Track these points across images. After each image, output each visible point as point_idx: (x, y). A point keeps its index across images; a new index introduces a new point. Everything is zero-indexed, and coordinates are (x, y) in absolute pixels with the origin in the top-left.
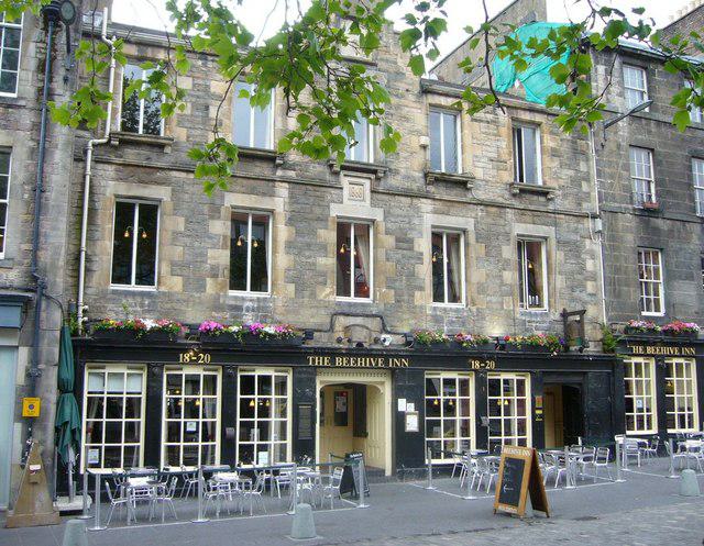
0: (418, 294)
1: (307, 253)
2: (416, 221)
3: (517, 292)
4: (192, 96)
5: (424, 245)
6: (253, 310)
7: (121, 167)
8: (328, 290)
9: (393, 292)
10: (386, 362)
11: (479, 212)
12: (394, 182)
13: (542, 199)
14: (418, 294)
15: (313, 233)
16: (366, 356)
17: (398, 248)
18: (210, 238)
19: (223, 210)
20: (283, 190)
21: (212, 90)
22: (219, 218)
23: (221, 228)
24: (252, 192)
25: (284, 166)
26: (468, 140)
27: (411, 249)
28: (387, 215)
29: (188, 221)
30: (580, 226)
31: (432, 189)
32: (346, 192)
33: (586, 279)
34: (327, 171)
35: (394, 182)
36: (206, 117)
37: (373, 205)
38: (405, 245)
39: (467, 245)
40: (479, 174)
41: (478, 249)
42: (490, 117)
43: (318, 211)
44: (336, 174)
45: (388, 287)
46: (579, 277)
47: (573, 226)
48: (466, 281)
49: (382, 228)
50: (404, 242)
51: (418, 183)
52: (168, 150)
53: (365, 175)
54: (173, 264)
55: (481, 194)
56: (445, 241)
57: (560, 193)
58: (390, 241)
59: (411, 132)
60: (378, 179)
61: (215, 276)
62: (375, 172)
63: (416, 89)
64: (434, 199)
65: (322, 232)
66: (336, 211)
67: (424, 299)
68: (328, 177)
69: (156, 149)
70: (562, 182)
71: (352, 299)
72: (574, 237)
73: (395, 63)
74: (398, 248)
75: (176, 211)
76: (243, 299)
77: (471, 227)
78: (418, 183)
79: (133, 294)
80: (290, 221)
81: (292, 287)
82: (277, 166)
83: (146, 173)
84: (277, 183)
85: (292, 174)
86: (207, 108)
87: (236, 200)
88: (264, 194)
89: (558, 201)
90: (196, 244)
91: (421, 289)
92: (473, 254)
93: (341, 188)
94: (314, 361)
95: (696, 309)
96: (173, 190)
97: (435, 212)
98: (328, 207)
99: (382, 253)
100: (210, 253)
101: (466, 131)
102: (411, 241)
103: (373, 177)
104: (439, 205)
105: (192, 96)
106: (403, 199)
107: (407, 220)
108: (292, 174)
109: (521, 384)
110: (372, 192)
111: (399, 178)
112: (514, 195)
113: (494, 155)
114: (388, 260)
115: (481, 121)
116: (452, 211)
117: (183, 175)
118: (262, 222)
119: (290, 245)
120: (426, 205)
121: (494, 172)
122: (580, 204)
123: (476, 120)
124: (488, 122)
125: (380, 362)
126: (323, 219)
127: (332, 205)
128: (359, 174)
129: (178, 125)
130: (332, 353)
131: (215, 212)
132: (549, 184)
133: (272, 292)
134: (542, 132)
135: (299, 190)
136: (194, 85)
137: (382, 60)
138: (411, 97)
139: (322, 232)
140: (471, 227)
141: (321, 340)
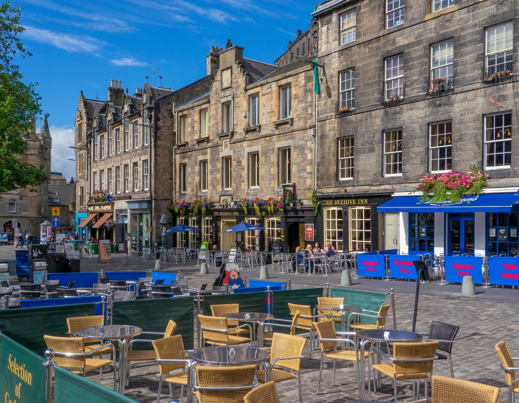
3: (276, 177)
12: (237, 137)
14: (243, 184)
27: (241, 165)
28: (234, 152)
30: (305, 135)
33: (307, 165)
36: (194, 130)
37: (231, 149)
42: (269, 90)
43: (216, 156)
46: (303, 164)
55: (264, 132)
56: (254, 156)
57: (296, 119)
70: (298, 113)
72: (302, 142)
89: (295, 124)
91: (244, 182)
95: (374, 172)
97: (248, 146)
102: (240, 162)
111: (238, 134)
113: (269, 110)
116: (254, 144)
120: (245, 144)
124: (268, 94)
138: (242, 96)
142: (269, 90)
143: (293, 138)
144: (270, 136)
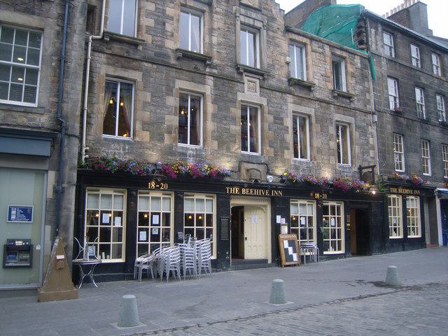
0: (286, 151)
1: (225, 122)
2: (284, 107)
4: (156, 15)
5: (289, 122)
6: (193, 156)
7: (110, 57)
8: (237, 146)
9: (272, 149)
10: (270, 193)
11: (317, 105)
12: (272, 82)
13: (348, 101)
14: (286, 151)
15: (228, 110)
16: (259, 188)
17: (275, 123)
18: (166, 108)
19: (174, 91)
20: (210, 81)
21: (167, 13)
22: (172, 95)
23: (173, 101)
24: (192, 80)
25: (211, 66)
26: (310, 62)
27: (282, 124)
29: (152, 96)
31: (292, 89)
32: (246, 85)
34: (235, 71)
35: (272, 82)
37: (261, 95)
38: (279, 122)
39: (311, 124)
40: (316, 82)
41: (317, 127)
43: (230, 96)
44: (241, 74)
45: (270, 147)
47: (363, 117)
48: (310, 145)
49: (266, 110)
50: (279, 119)
51: (285, 85)
52: (140, 48)
53: (257, 76)
54: (144, 123)
55: (317, 95)
56: (301, 121)
58: (270, 118)
59: (281, 54)
60: (264, 79)
61: (170, 133)
62: (262, 75)
63: (282, 28)
64: (294, 95)
65: (233, 109)
66: (240, 97)
67: (289, 154)
68: (236, 75)
69: (133, 47)
71: (249, 152)
73: (272, 12)
74: (275, 123)
75: (145, 88)
76: (187, 149)
77: (313, 114)
78: (285, 85)
79: (118, 142)
80: (214, 102)
81: (216, 143)
82: (206, 66)
83: (126, 61)
84: (207, 77)
85: (215, 71)
86: (164, 24)
87: (182, 84)
88: (199, 83)
89: (355, 103)
90: (158, 111)
91: (288, 149)
92: (314, 130)
93: (244, 83)
94: (230, 190)
96: (143, 75)
97: (294, 103)
98: (236, 94)
99: (266, 125)
100: (167, 117)
101: (309, 57)
102: (282, 119)
103: (261, 78)
104: (296, 99)
105: (156, 15)
106: (277, 93)
107: (279, 106)
108: (215, 71)
109: (339, 208)
110: (261, 87)
112: (334, 97)
114: (270, 129)
115: (316, 52)
117: (150, 65)
118: (196, 100)
119: (214, 116)
120: (290, 98)
121: (323, 83)
122: (365, 106)
123: (314, 51)
125: (267, 193)
126: (234, 101)
127: (238, 93)
128: (254, 76)
129: (146, 33)
130: (241, 186)
131: (170, 91)
132: (350, 92)
133: (204, 145)
134: (346, 63)
135: (220, 82)
136: (156, 8)
137: (264, 8)
138: (280, 33)
139: (233, 109)
140: (313, 114)
141: (235, 178)
142: (321, 50)
143: (355, 116)
144: (328, 103)
